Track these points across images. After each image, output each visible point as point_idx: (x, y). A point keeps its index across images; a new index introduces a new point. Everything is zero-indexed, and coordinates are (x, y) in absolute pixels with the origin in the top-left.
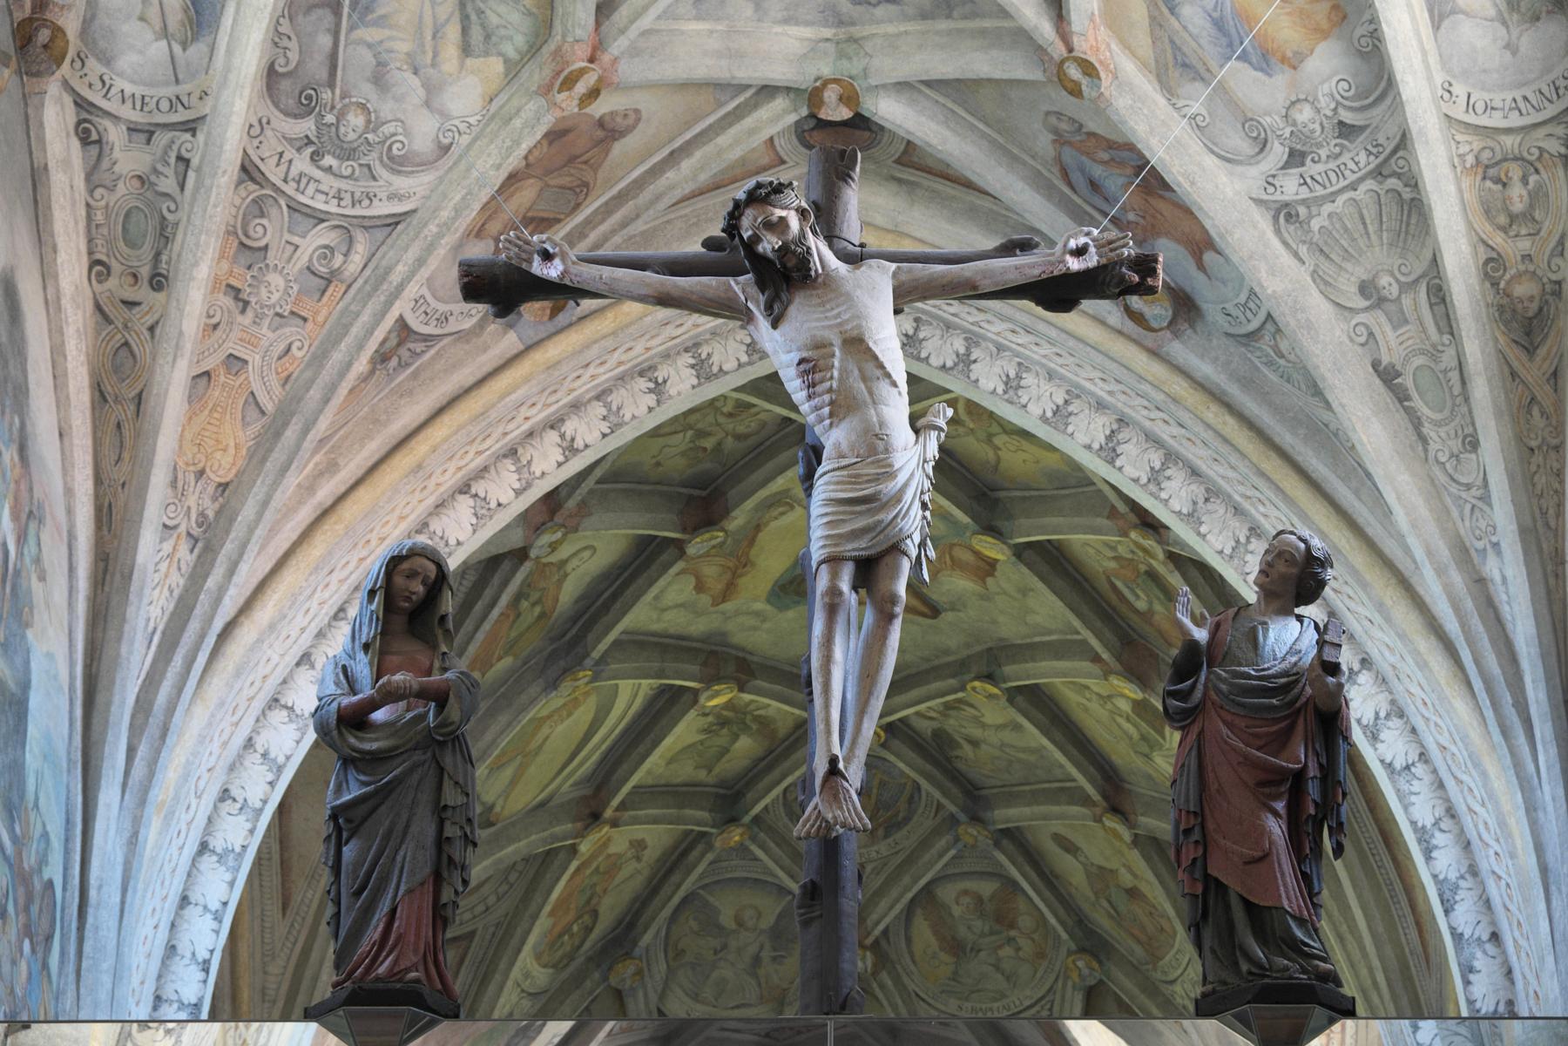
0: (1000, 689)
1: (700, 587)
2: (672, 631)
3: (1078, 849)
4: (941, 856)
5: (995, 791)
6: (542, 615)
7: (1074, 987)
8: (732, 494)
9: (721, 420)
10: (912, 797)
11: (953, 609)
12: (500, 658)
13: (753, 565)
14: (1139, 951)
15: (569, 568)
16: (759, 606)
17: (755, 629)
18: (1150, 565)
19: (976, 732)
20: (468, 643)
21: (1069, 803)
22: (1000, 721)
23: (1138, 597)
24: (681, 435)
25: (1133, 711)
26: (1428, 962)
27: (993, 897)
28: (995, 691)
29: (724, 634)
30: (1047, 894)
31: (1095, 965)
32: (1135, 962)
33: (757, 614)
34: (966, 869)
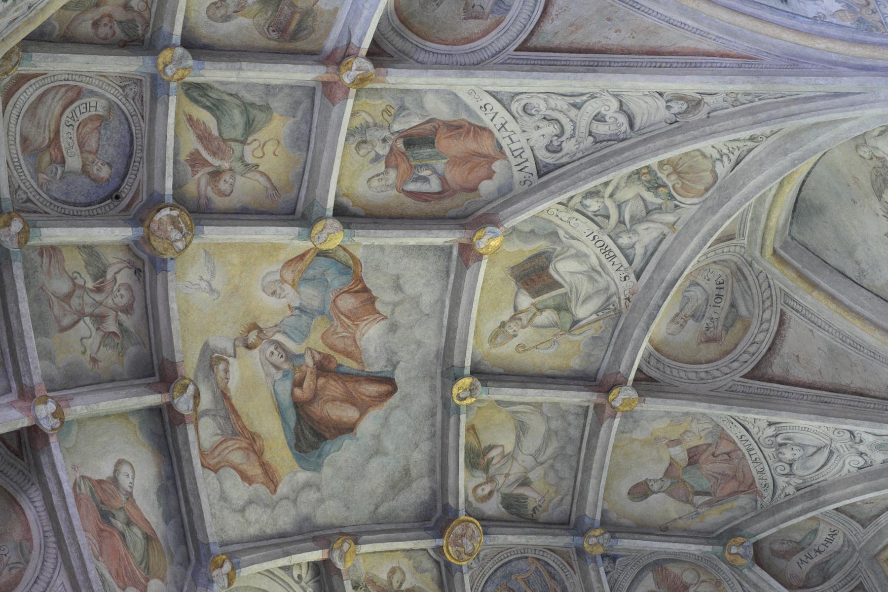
0: (467, 376)
1: (246, 478)
2: (269, 531)
3: (645, 483)
4: (600, 581)
5: (574, 509)
6: (149, 538)
7: (750, 569)
8: (165, 353)
9: (98, 297)
10: (550, 573)
11: (395, 366)
12: (147, 580)
13: (259, 436)
14: (743, 500)
15: (125, 482)
16: (303, 476)
17: (321, 501)
18: (402, 134)
19: (516, 470)
20: (71, 522)
21: (598, 438)
22: (512, 438)
23: (425, 179)
24: (82, 322)
25: (534, 297)
26: (752, 58)
27: (657, 584)
28: (467, 381)
29: (307, 519)
30: (673, 539)
31: (740, 540)
32: (753, 514)
33: (308, 485)
34: (627, 585)
